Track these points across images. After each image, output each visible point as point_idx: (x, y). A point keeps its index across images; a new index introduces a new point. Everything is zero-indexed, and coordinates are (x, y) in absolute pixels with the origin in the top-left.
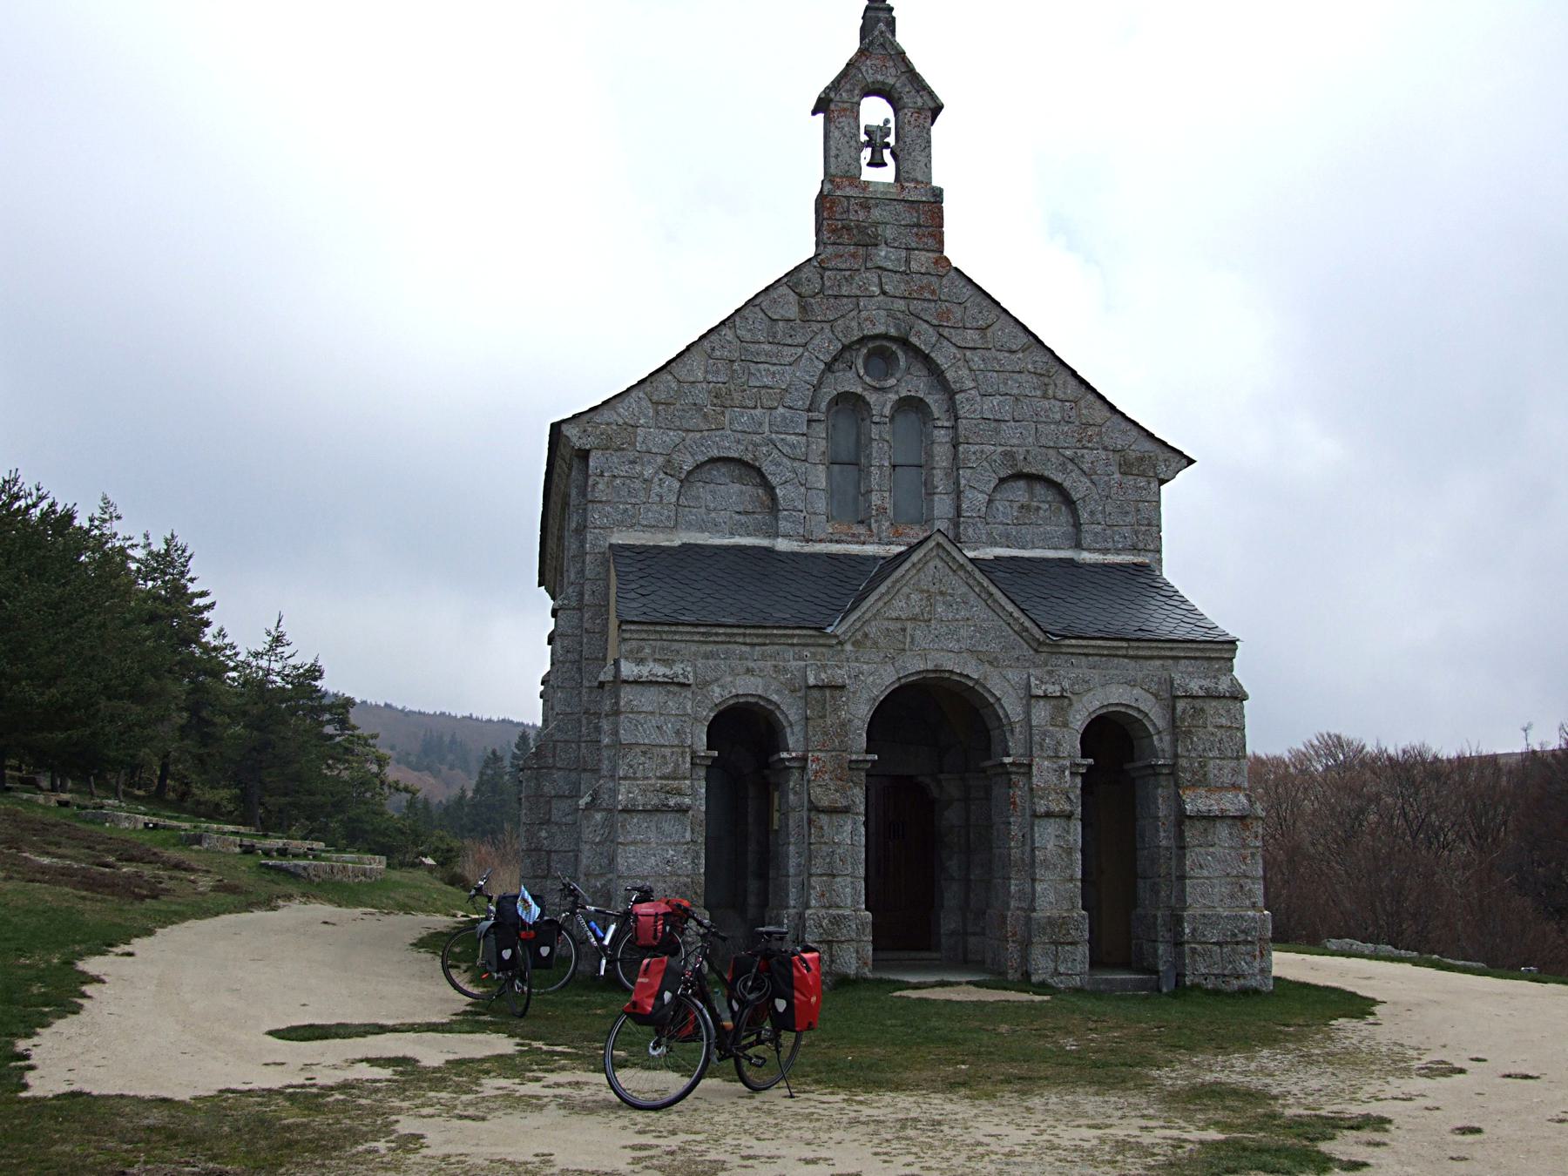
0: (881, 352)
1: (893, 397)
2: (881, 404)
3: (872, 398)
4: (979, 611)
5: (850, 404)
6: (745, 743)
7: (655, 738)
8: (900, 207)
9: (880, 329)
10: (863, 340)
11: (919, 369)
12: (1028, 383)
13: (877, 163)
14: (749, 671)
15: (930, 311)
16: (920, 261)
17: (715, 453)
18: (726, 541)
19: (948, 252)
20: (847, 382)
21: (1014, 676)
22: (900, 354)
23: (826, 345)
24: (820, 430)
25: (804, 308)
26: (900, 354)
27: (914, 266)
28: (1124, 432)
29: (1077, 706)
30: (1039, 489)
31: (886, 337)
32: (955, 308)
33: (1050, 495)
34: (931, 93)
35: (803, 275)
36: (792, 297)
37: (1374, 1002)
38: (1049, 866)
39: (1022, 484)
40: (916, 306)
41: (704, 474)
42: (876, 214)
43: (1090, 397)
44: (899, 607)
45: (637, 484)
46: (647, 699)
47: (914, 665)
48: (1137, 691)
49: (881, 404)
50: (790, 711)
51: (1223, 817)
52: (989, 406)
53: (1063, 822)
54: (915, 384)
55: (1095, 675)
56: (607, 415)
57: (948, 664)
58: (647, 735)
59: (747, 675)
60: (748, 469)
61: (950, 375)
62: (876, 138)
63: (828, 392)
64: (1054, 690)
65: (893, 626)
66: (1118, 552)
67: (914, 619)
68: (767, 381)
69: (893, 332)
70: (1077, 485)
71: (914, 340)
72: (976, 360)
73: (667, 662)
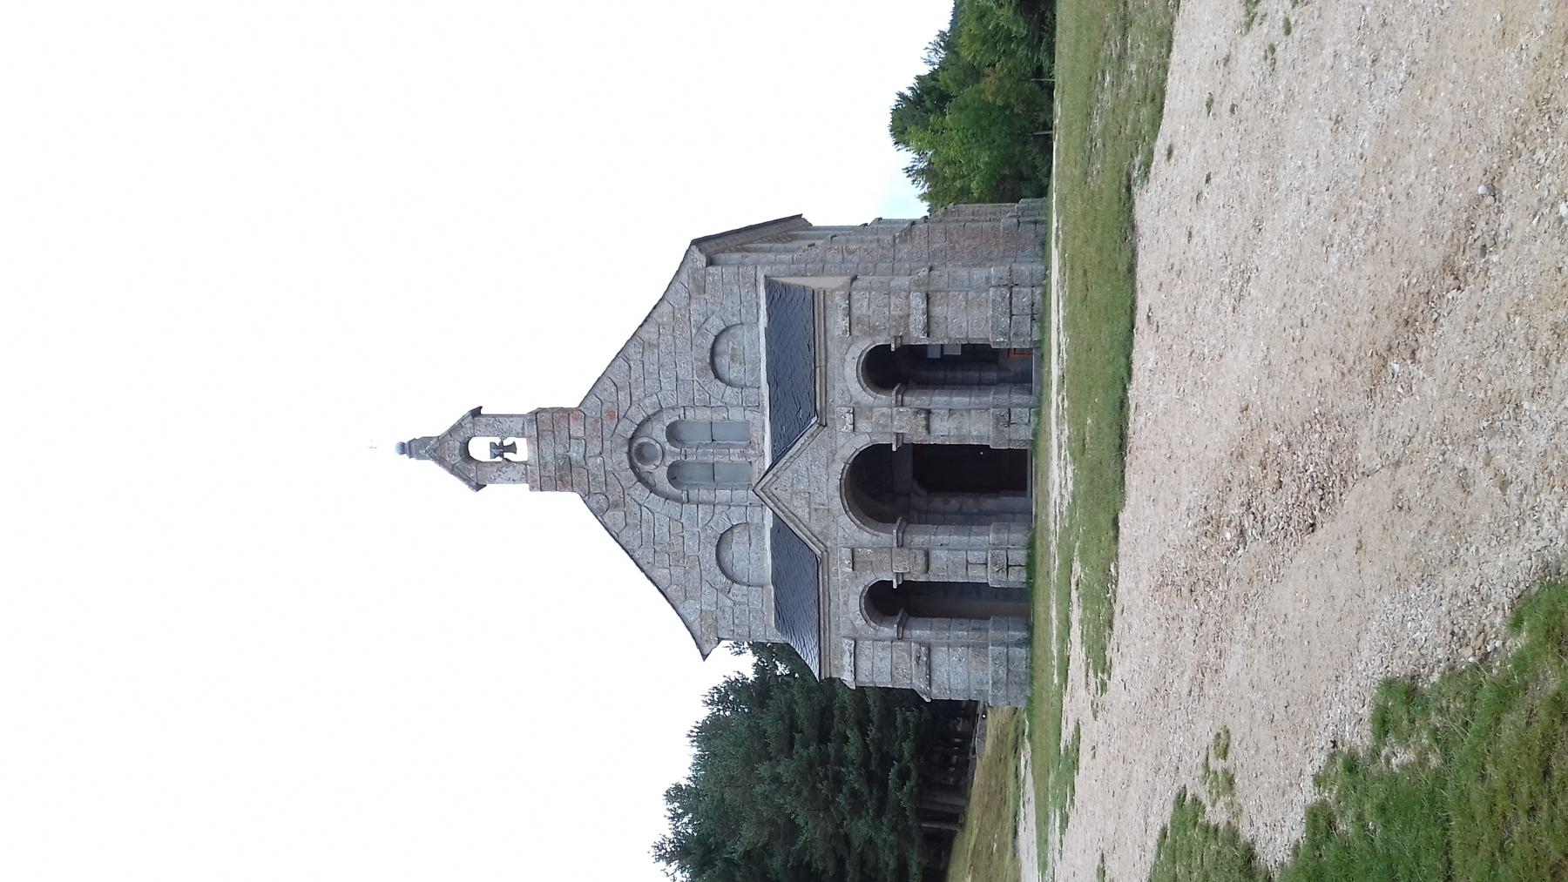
0: (638, 454)
1: (668, 446)
2: (673, 453)
3: (669, 460)
4: (801, 463)
5: (674, 475)
6: (888, 602)
7: (887, 663)
8: (542, 443)
9: (625, 457)
10: (633, 467)
11: (648, 428)
12: (652, 357)
13: (512, 448)
14: (845, 603)
15: (609, 424)
16: (577, 429)
17: (714, 562)
18: (769, 554)
19: (572, 401)
20: (660, 475)
21: (841, 440)
22: (640, 441)
23: (639, 491)
24: (694, 493)
25: (616, 505)
26: (640, 441)
27: (581, 434)
28: (677, 292)
29: (859, 398)
30: (720, 348)
31: (629, 453)
32: (605, 407)
33: (723, 340)
34: (463, 419)
35: (595, 506)
36: (610, 513)
37: (1180, 799)
38: (960, 420)
39: (717, 360)
40: (607, 435)
41: (727, 565)
42: (549, 458)
43: (655, 315)
44: (803, 513)
45: (737, 609)
46: (864, 665)
47: (837, 504)
48: (848, 358)
49: (673, 453)
50: (870, 578)
51: (928, 313)
52: (668, 385)
53: (933, 417)
54: (658, 432)
55: (839, 386)
56: (696, 627)
57: (835, 481)
58: (885, 666)
59: (847, 605)
60: (722, 541)
61: (650, 412)
62: (499, 450)
63: (668, 488)
64: (849, 418)
65: (814, 516)
66: (757, 296)
67: (809, 504)
68: (665, 530)
69: (626, 449)
70: (715, 325)
71: (629, 435)
72: (638, 393)
73: (843, 653)
